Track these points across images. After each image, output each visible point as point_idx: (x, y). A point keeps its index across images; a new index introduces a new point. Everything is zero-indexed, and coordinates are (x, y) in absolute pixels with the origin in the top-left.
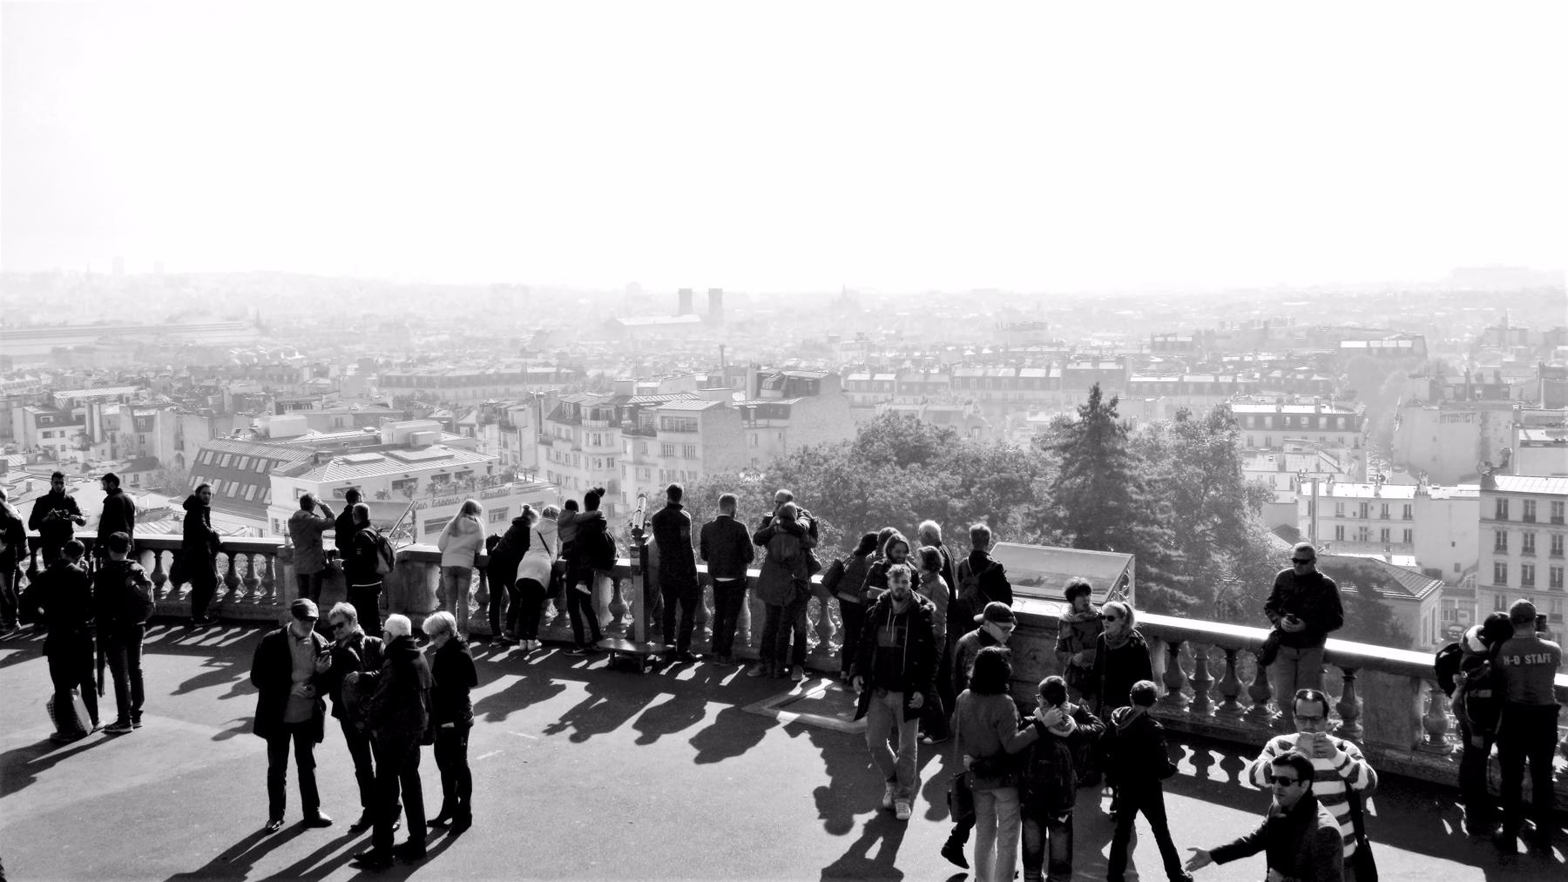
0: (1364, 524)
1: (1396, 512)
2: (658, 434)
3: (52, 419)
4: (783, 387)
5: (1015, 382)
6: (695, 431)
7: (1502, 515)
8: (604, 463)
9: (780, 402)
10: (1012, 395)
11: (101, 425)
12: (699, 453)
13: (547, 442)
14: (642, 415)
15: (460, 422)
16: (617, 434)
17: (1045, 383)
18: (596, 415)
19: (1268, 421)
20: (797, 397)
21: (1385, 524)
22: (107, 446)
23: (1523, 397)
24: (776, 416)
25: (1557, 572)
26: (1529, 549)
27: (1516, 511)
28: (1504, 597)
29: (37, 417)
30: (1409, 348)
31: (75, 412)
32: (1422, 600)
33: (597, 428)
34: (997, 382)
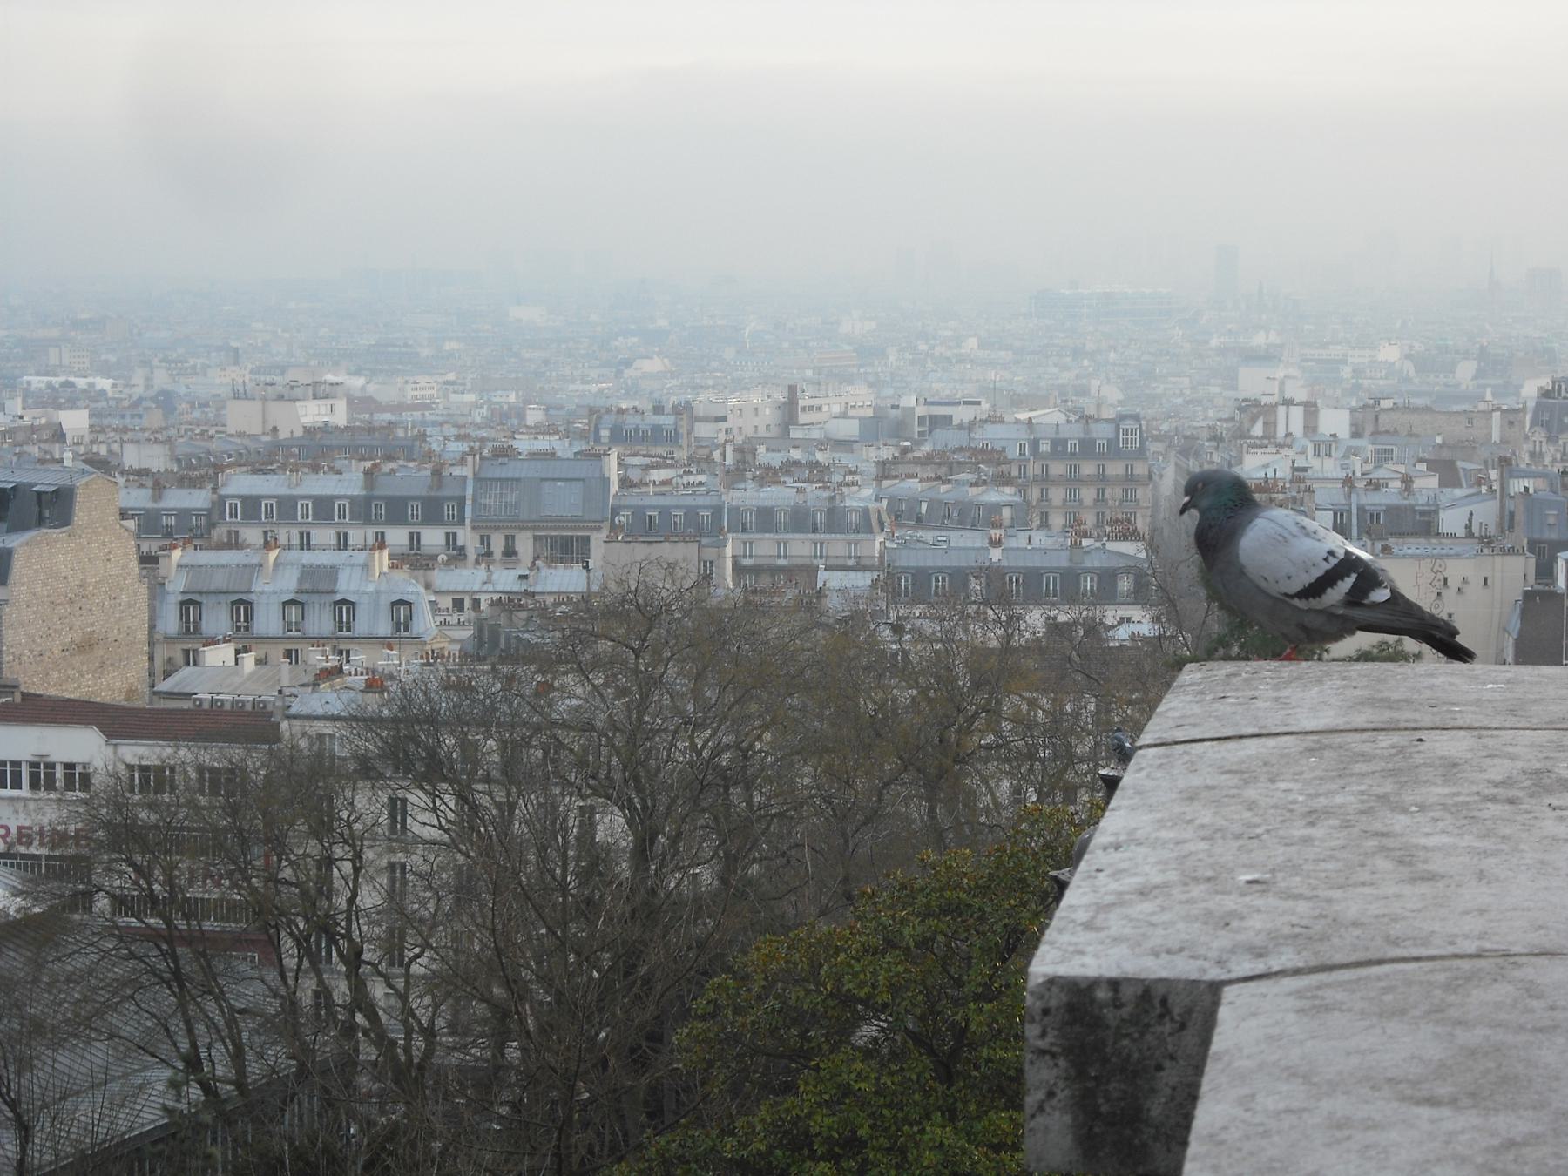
23: (1475, 529)
30: (1108, 440)
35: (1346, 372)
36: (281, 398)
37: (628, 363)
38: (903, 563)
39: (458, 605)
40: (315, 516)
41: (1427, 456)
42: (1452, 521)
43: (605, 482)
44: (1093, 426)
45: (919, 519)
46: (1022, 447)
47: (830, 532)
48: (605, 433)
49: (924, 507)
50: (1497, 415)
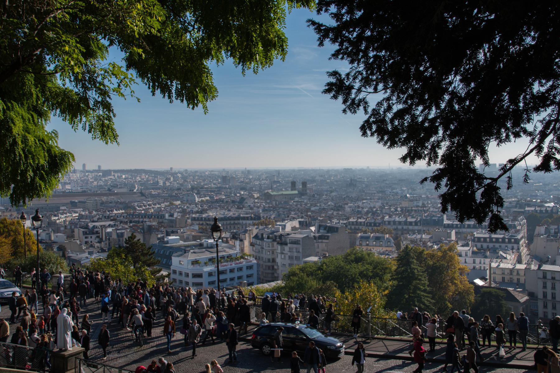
0: (511, 276)
1: (522, 273)
3: (88, 232)
4: (327, 229)
5: (406, 223)
6: (300, 244)
7: (545, 277)
10: (405, 227)
11: (105, 235)
12: (301, 250)
14: (283, 239)
17: (416, 223)
18: (268, 238)
19: (488, 240)
21: (518, 277)
22: (107, 242)
24: (324, 239)
28: (546, 302)
29: (83, 232)
31: (96, 230)
33: (269, 242)
34: (400, 223)
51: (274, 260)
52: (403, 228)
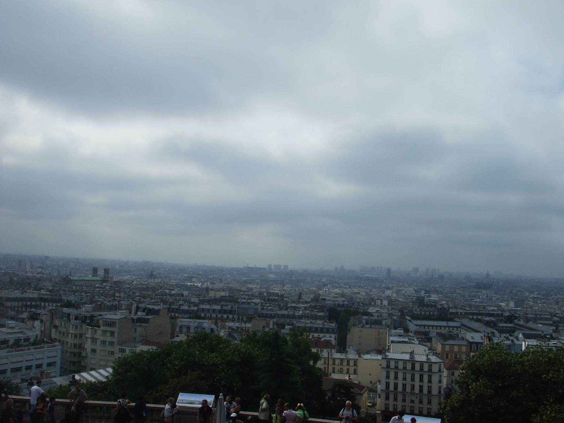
0: (341, 367)
2: (101, 327)
4: (146, 311)
7: (388, 366)
8: (78, 336)
9: (146, 317)
10: (219, 316)
13: (56, 327)
15: (19, 317)
16: (84, 326)
17: (231, 312)
18: (76, 318)
20: (152, 315)
23: (387, 323)
25: (404, 385)
26: (396, 378)
27: (392, 365)
32: (363, 394)
34: (214, 311)
35: (403, 292)
36: (218, 291)
37: (285, 285)
38: (296, 325)
39: (229, 328)
40: (213, 312)
41: (398, 309)
42: (384, 322)
43: (258, 309)
44: (345, 302)
45: (308, 317)
46: (333, 305)
47: (292, 319)
48: (266, 299)
49: (309, 315)
50: (411, 303)
51: (81, 346)
52: (217, 316)
